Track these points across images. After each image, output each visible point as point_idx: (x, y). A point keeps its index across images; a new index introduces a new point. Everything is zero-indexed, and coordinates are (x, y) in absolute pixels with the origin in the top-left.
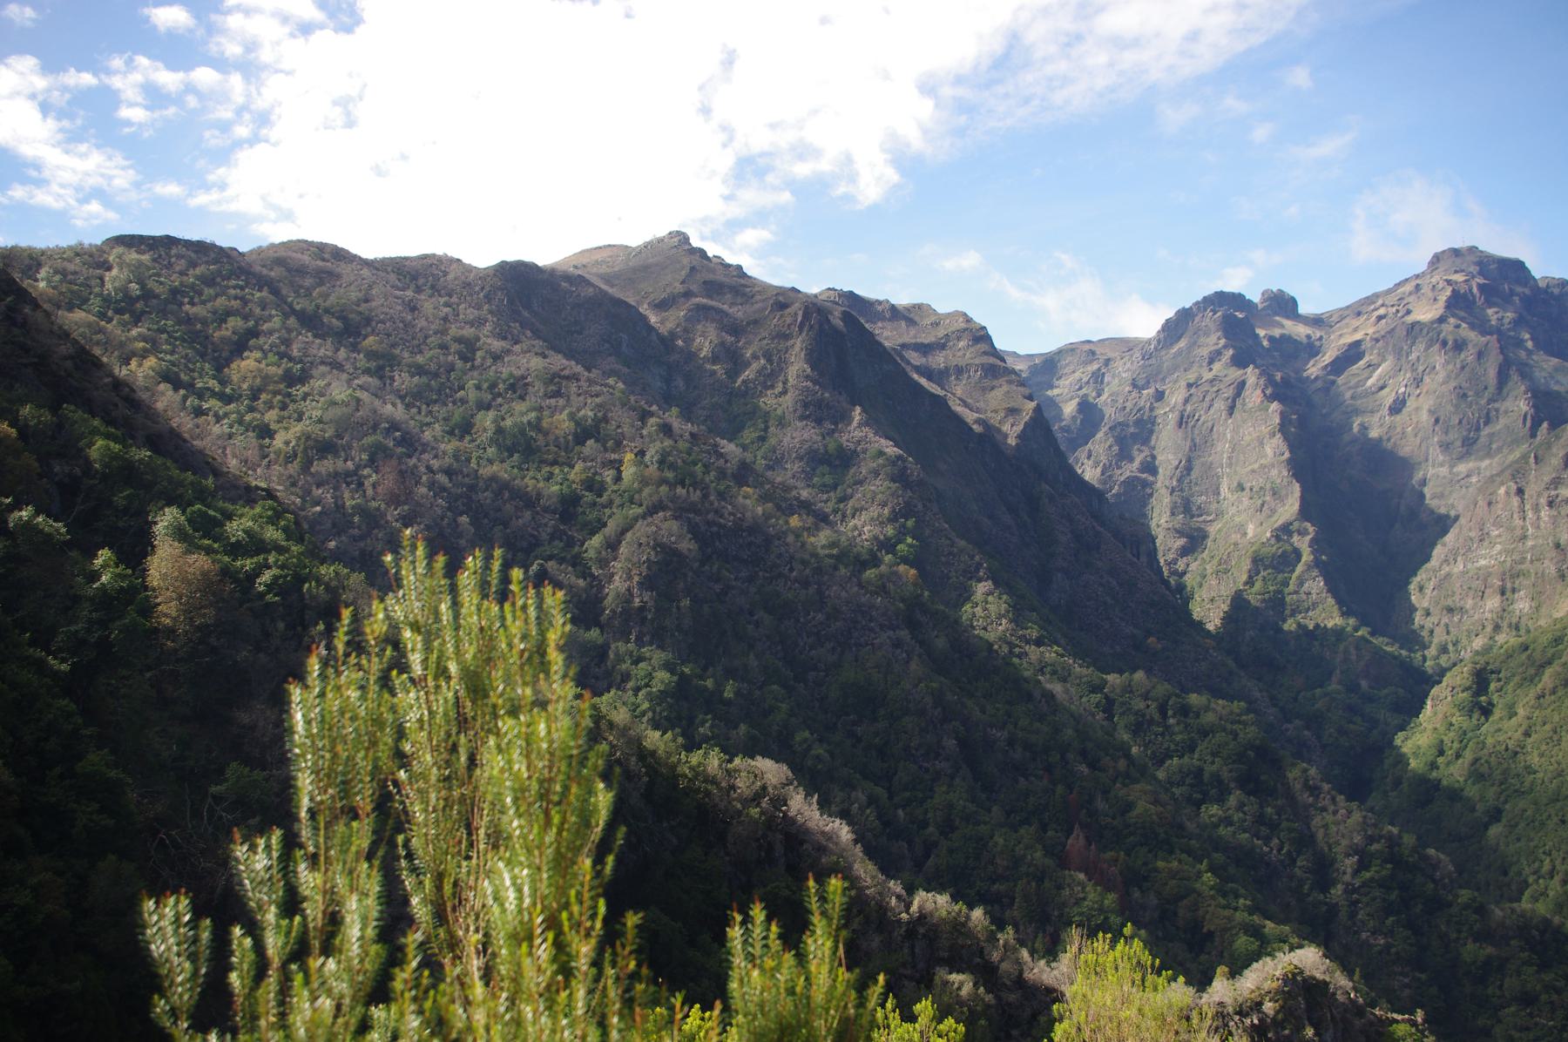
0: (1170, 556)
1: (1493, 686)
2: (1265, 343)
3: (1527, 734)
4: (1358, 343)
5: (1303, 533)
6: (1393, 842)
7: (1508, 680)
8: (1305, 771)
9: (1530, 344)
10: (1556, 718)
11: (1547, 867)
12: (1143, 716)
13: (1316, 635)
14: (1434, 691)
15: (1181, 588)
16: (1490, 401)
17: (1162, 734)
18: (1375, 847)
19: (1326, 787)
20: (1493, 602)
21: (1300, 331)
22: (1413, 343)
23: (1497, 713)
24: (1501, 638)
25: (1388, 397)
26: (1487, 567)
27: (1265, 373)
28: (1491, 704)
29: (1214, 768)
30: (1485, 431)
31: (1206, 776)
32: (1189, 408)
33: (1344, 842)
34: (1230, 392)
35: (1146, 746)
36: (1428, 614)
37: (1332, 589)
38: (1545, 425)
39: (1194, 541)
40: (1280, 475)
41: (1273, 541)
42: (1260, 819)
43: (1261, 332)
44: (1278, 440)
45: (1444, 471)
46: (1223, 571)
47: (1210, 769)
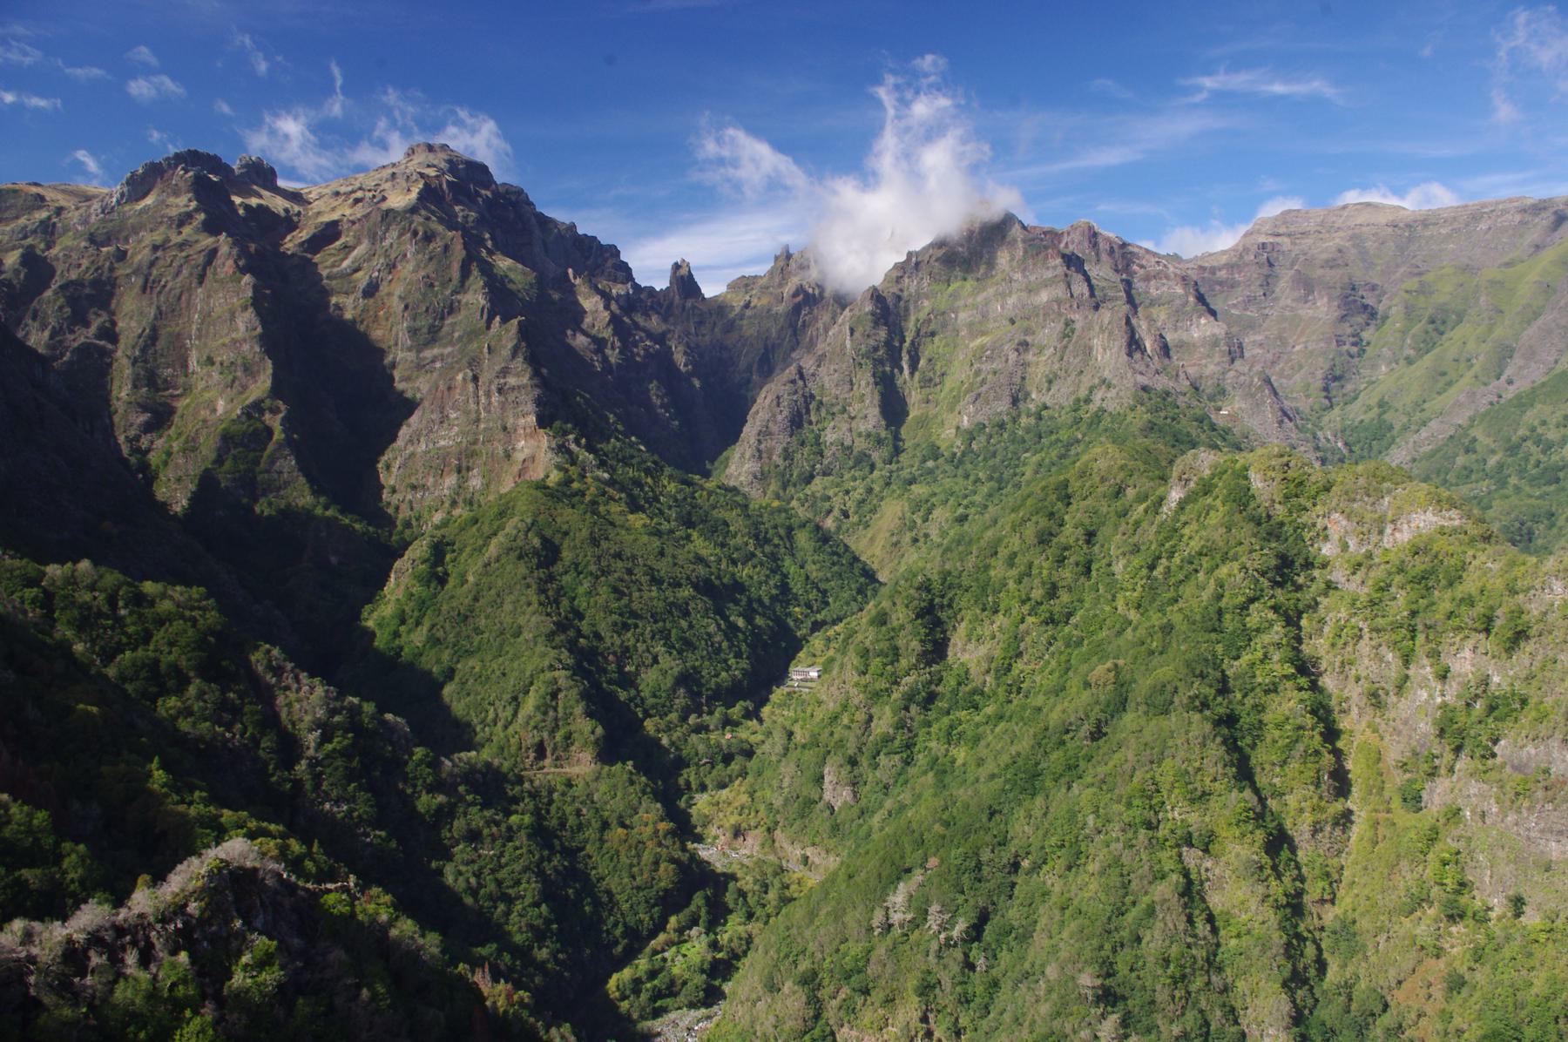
0: (132, 433)
1: (448, 557)
2: (241, 212)
3: (476, 599)
4: (335, 223)
5: (275, 411)
6: (354, 712)
7: (461, 551)
8: (268, 651)
9: (489, 244)
10: (500, 583)
11: (491, 715)
12: (90, 608)
13: (288, 515)
14: (397, 564)
15: (144, 466)
16: (455, 292)
17: (112, 628)
18: (337, 719)
19: (289, 666)
20: (451, 480)
21: (279, 204)
22: (387, 230)
23: (452, 582)
24: (456, 512)
25: (362, 279)
26: (444, 447)
27: (239, 242)
28: (446, 574)
29: (172, 658)
30: (448, 322)
31: (163, 667)
32: (155, 272)
33: (308, 718)
34: (201, 259)
35: (93, 641)
36: (394, 491)
37: (304, 469)
38: (498, 318)
39: (160, 417)
40: (251, 350)
41: (244, 418)
42: (223, 705)
43: (237, 200)
44: (250, 314)
45: (411, 356)
46: (191, 448)
47: (167, 659)
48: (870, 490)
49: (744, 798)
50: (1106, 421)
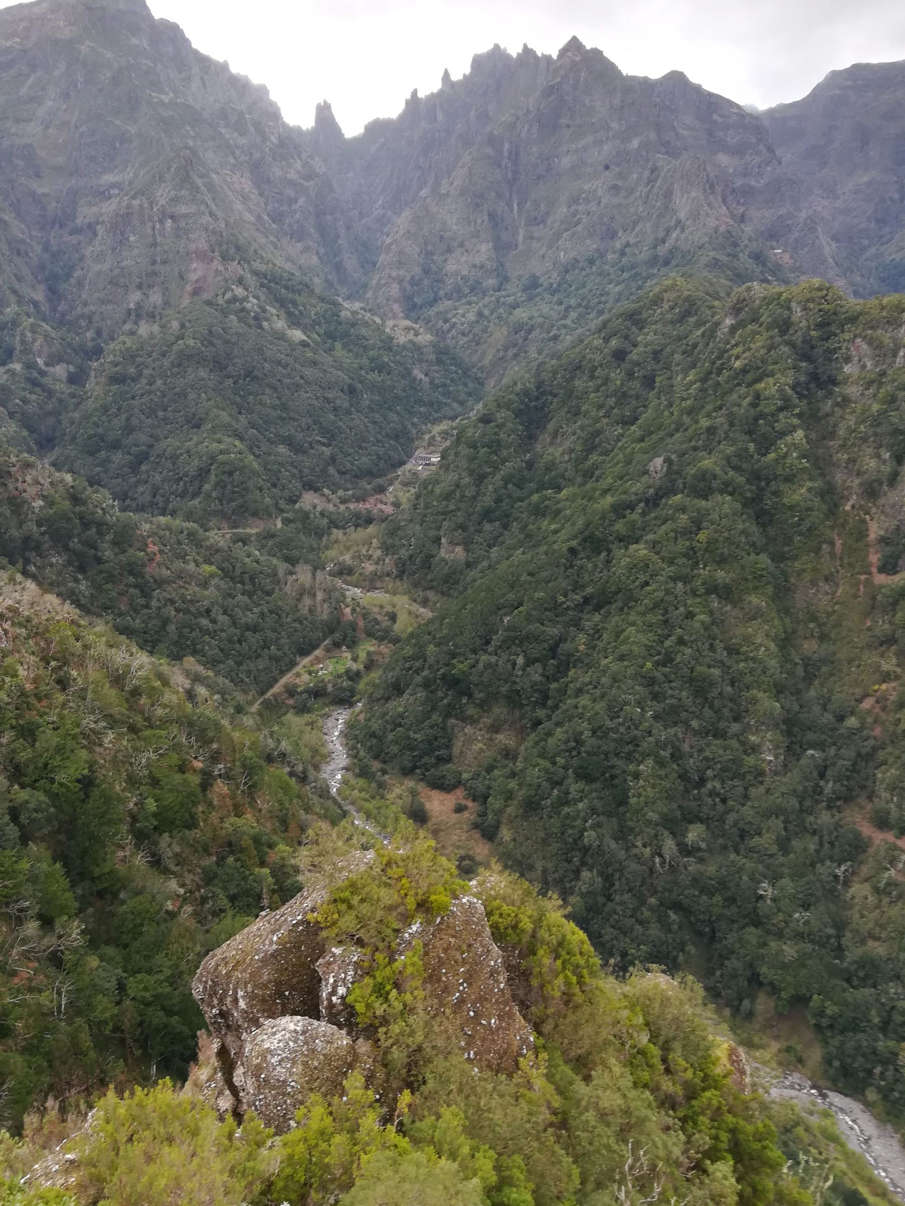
49: (378, 553)
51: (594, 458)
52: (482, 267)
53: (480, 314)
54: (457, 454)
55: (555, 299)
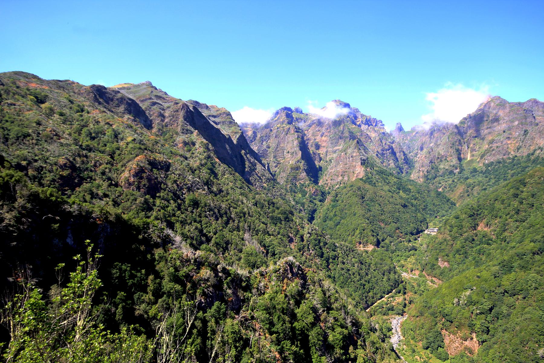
23: (340, 201)
40: (297, 149)
45: (331, 149)
48: (453, 181)
49: (414, 261)
50: (540, 160)
51: (506, 234)
52: (453, 166)
53: (453, 181)
54: (445, 229)
55: (484, 176)
